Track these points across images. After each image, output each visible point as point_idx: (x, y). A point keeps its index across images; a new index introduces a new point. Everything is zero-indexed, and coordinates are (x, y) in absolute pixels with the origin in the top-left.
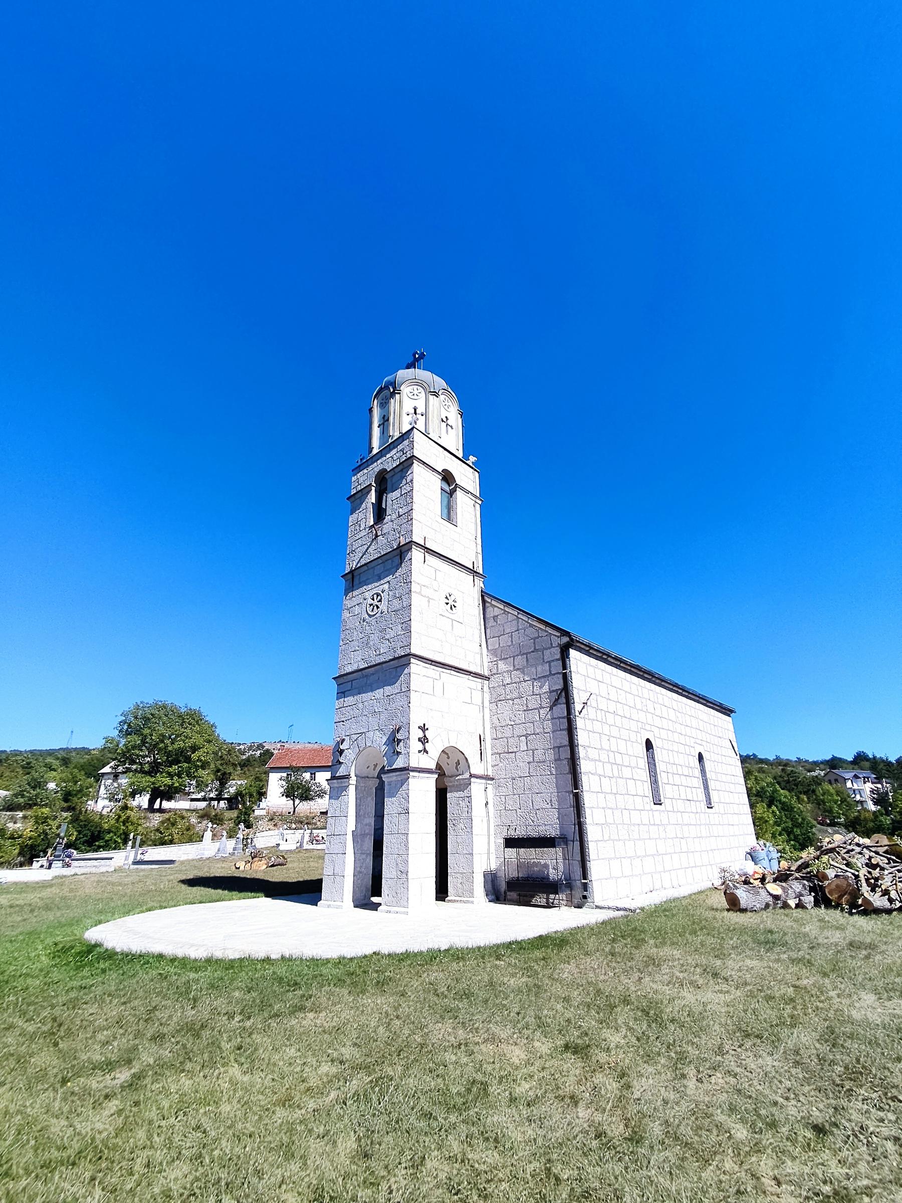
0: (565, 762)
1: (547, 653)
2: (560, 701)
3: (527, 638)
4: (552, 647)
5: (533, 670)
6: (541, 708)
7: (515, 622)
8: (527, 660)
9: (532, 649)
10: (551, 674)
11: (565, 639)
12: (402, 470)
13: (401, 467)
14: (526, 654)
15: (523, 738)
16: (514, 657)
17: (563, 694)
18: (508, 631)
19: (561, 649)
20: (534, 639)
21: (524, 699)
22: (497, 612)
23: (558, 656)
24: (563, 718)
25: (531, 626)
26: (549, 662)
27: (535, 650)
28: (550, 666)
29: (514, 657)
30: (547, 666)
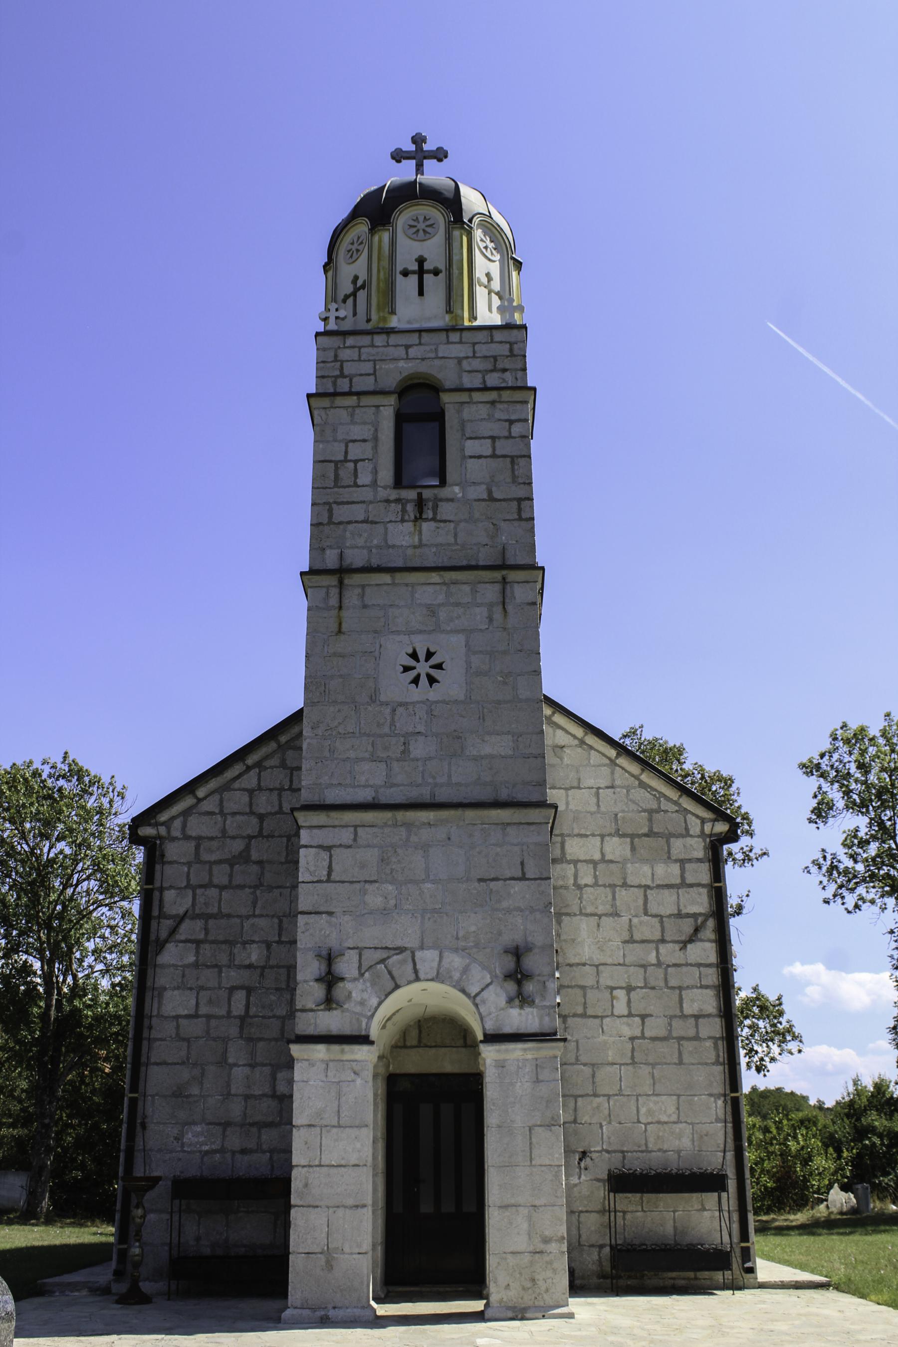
0: (709, 1044)
1: (677, 845)
2: (701, 935)
3: (633, 807)
4: (687, 834)
5: (646, 869)
6: (663, 941)
7: (606, 771)
8: (633, 849)
9: (645, 830)
10: (684, 884)
11: (722, 827)
12: (493, 403)
13: (493, 395)
14: (632, 836)
15: (621, 994)
16: (602, 837)
17: (711, 923)
18: (590, 782)
19: (711, 841)
20: (651, 812)
21: (625, 919)
22: (561, 738)
23: (700, 854)
24: (709, 965)
25: (643, 785)
26: (682, 862)
27: (650, 834)
28: (683, 870)
29: (602, 837)
30: (675, 869)
